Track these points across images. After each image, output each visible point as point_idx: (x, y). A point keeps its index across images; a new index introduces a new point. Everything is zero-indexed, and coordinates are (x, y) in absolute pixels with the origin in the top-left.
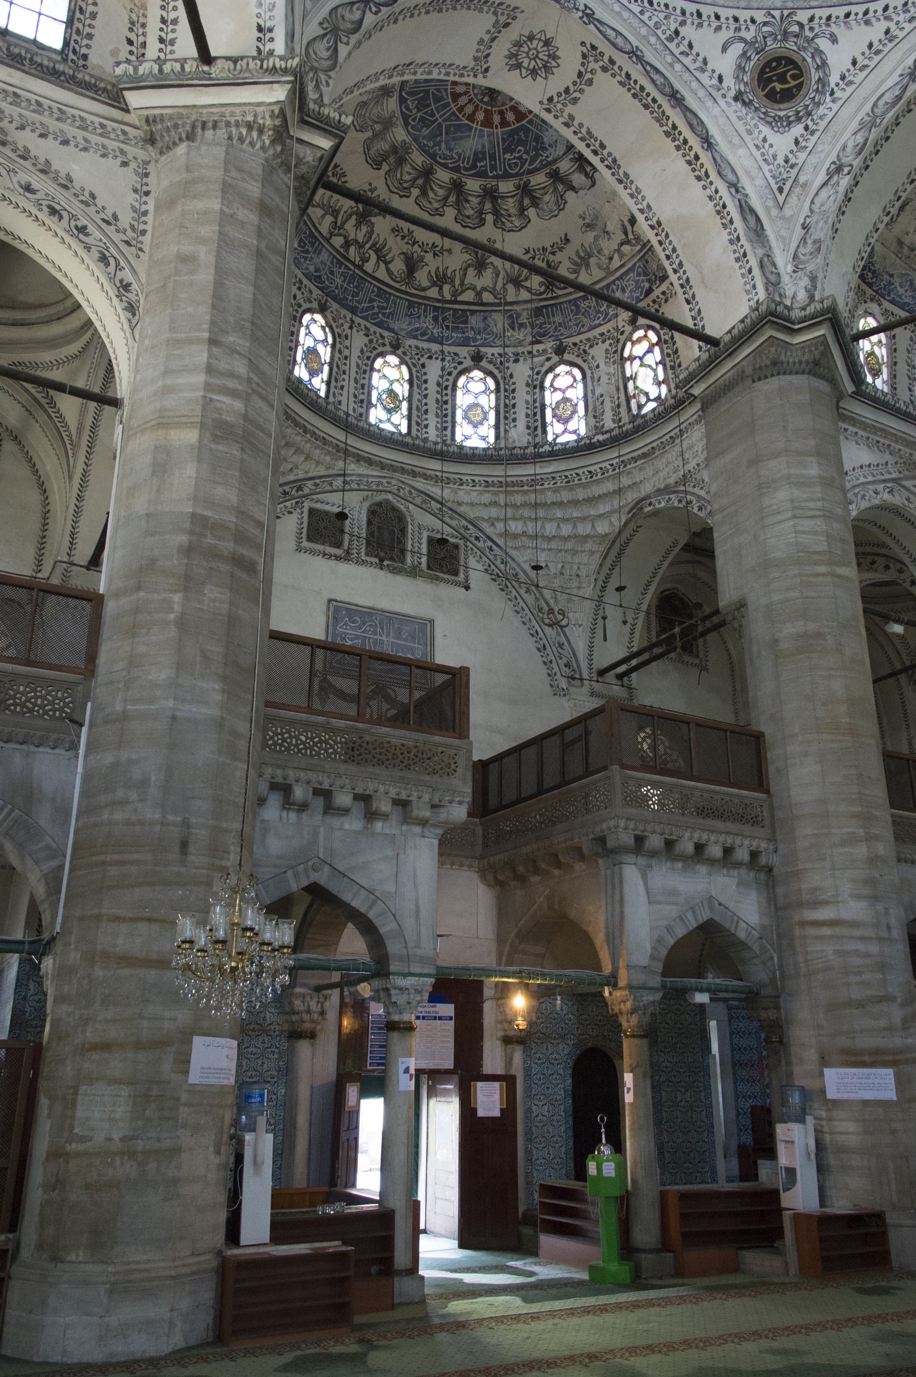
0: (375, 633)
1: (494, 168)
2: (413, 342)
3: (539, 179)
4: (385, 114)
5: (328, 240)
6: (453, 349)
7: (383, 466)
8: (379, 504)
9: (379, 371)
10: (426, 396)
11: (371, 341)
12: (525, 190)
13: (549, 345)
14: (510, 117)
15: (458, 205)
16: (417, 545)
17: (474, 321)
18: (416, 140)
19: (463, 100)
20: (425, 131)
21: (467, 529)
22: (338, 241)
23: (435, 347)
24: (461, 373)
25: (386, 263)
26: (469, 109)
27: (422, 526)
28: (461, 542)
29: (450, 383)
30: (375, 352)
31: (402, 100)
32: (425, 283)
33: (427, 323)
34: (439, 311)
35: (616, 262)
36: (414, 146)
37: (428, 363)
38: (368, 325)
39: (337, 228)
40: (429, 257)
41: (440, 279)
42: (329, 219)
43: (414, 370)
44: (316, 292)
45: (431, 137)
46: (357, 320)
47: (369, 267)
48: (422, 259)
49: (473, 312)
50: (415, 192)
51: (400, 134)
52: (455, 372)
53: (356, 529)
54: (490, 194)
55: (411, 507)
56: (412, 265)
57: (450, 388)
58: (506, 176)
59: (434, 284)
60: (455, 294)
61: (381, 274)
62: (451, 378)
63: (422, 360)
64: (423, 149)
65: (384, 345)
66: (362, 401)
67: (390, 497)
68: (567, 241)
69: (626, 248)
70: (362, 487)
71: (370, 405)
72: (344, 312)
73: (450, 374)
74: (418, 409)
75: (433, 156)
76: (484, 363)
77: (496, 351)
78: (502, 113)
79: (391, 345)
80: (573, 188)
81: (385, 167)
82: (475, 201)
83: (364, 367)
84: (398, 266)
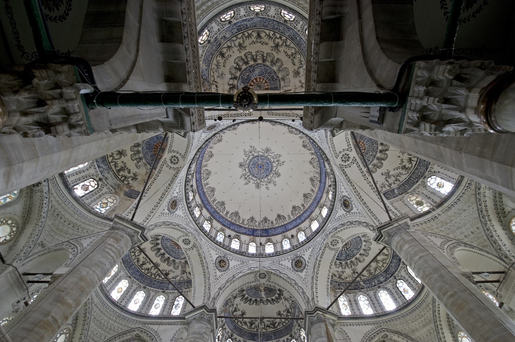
1: (249, 69)
2: (251, 17)
3: (238, 74)
4: (280, 73)
5: (287, 38)
6: (238, 20)
12: (240, 69)
13: (212, 40)
14: (252, 83)
15: (253, 56)
17: (236, 30)
18: (270, 68)
19: (264, 82)
20: (269, 71)
22: (284, 38)
23: (244, 18)
24: (234, 16)
25: (267, 35)
26: (261, 80)
31: (278, 77)
32: (253, 33)
33: (248, 24)
34: (247, 28)
35: (212, 74)
36: (270, 66)
37: (245, 14)
39: (285, 42)
40: (255, 40)
41: (250, 36)
42: (288, 44)
44: (289, 25)
45: (267, 70)
46: (272, 18)
47: (272, 33)
48: (256, 39)
49: (237, 32)
50: (265, 55)
51: (275, 68)
54: (246, 63)
56: (259, 36)
58: (245, 69)
59: (250, 34)
60: (244, 34)
61: (267, 32)
64: (268, 66)
68: (224, 66)
69: (213, 79)
72: (278, 20)
75: (264, 65)
76: (227, 23)
77: (225, 27)
78: (254, 83)
80: (231, 79)
81: (275, 59)
82: (249, 59)
84: (263, 35)
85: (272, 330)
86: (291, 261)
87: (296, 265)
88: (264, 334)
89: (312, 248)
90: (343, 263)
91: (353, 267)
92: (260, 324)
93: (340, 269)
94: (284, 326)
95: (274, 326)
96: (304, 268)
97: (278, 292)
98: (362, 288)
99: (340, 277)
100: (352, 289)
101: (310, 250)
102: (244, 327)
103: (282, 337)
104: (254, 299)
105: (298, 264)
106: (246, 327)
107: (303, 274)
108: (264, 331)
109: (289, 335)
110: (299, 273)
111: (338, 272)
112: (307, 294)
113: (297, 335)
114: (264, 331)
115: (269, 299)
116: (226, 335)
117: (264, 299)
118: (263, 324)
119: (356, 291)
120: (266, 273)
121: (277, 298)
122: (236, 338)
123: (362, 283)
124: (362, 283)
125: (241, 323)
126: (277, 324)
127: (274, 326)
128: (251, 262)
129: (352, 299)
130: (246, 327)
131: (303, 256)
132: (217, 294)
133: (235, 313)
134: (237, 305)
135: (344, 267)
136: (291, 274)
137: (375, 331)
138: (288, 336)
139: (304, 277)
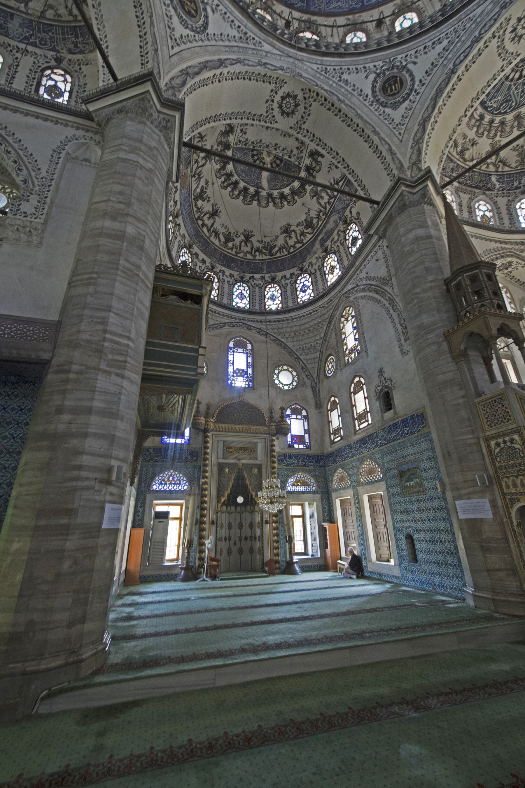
85: (265, 257)
86: (372, 76)
87: (384, 89)
88: (248, 262)
89: (445, 42)
90: (488, 118)
91: (498, 138)
92: (243, 244)
93: (471, 134)
94: (289, 253)
95: (270, 252)
96: (405, 100)
97: (303, 174)
98: (489, 190)
99: (461, 153)
100: (470, 186)
101: (439, 48)
102: (213, 239)
103: (282, 271)
104: (242, 185)
105: (392, 86)
106: (217, 242)
107: (397, 115)
108: (249, 256)
109: (296, 268)
110: (388, 110)
111: (465, 137)
112: (399, 155)
113: (316, 267)
114: (249, 256)
115: (275, 193)
116: (179, 238)
117: (264, 193)
118: (249, 245)
119: (477, 191)
120: (300, 97)
121: (293, 192)
122: (196, 254)
123: (494, 179)
124: (494, 179)
125: (209, 230)
126: (277, 249)
127: (270, 252)
128: (266, 47)
129: (465, 203)
130: (217, 242)
131: (410, 66)
132: (178, 81)
133: (200, 203)
134: (207, 183)
135: (481, 131)
136: (365, 109)
137: (498, 252)
138: (295, 270)
139: (397, 120)
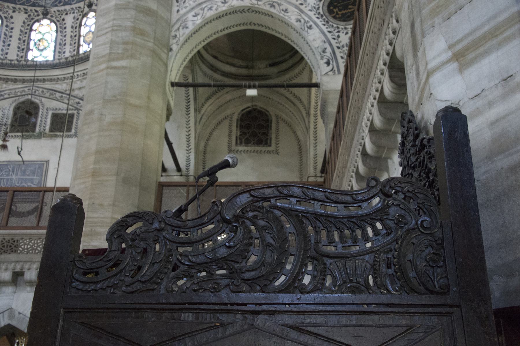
0: (8, 175)
2: (55, 9)
7: (24, 81)
8: (23, 103)
9: (35, 30)
10: (65, 36)
11: (29, 16)
16: (44, 121)
21: (79, 103)
23: (68, 7)
27: (49, 107)
28: (75, 112)
29: (78, 25)
30: (33, 21)
38: (26, 7)
43: (58, 23)
46: (17, 6)
52: (80, 17)
53: (5, 119)
55: (43, 100)
57: (78, 28)
62: (78, 22)
63: (63, 17)
65: (38, 15)
66: (23, 49)
67: (30, 97)
70: (11, 96)
71: (28, 49)
73: (78, 19)
74: (60, 44)
79: (43, 14)
83: (26, 31)
